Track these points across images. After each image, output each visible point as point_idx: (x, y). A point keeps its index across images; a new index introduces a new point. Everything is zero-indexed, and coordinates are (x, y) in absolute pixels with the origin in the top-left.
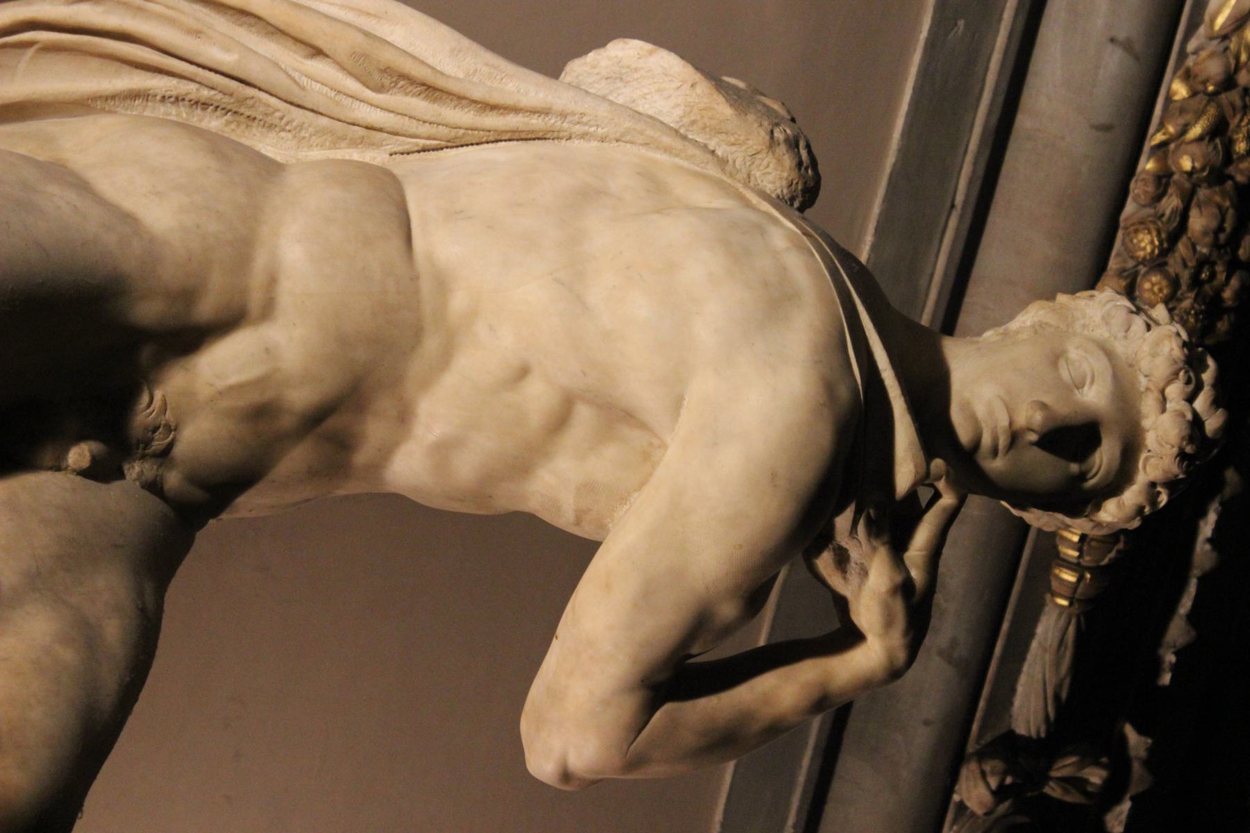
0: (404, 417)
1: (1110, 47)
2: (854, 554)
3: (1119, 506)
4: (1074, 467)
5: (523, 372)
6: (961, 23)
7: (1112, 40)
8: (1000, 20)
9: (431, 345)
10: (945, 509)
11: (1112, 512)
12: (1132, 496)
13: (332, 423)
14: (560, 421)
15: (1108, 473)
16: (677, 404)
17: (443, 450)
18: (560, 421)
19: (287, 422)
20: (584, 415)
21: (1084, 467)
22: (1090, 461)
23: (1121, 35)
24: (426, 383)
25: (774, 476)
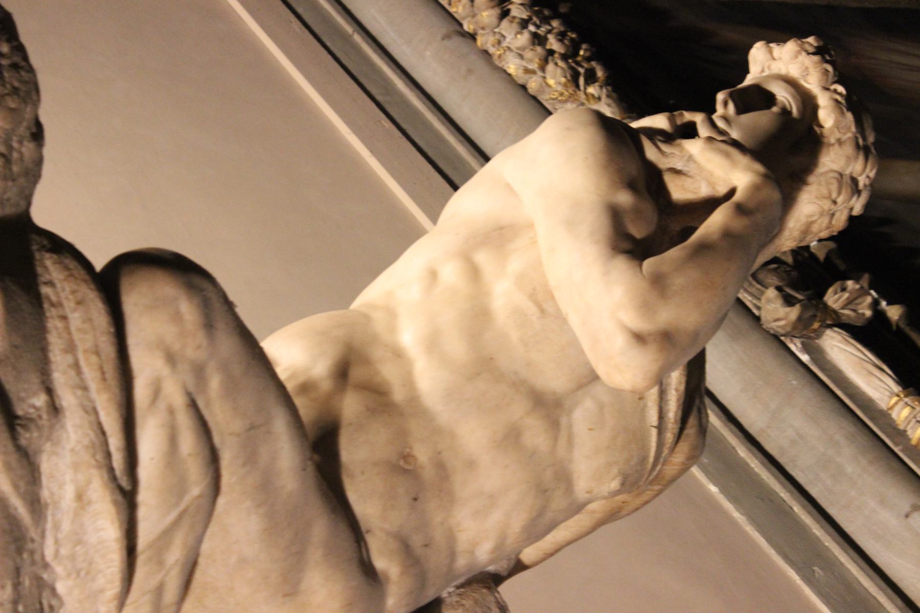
0: (398, 354)
1: (910, 520)
2: (679, 166)
3: (825, 107)
4: (775, 109)
5: (433, 275)
6: (816, 568)
7: (907, 516)
8: (842, 564)
9: (378, 317)
10: (703, 121)
11: (827, 117)
12: (824, 101)
13: (357, 373)
14: (474, 273)
15: (793, 97)
16: (508, 187)
17: (433, 343)
18: (474, 273)
19: (326, 385)
20: (482, 258)
21: (780, 106)
22: (778, 101)
23: (906, 508)
24: (393, 329)
25: (568, 129)
